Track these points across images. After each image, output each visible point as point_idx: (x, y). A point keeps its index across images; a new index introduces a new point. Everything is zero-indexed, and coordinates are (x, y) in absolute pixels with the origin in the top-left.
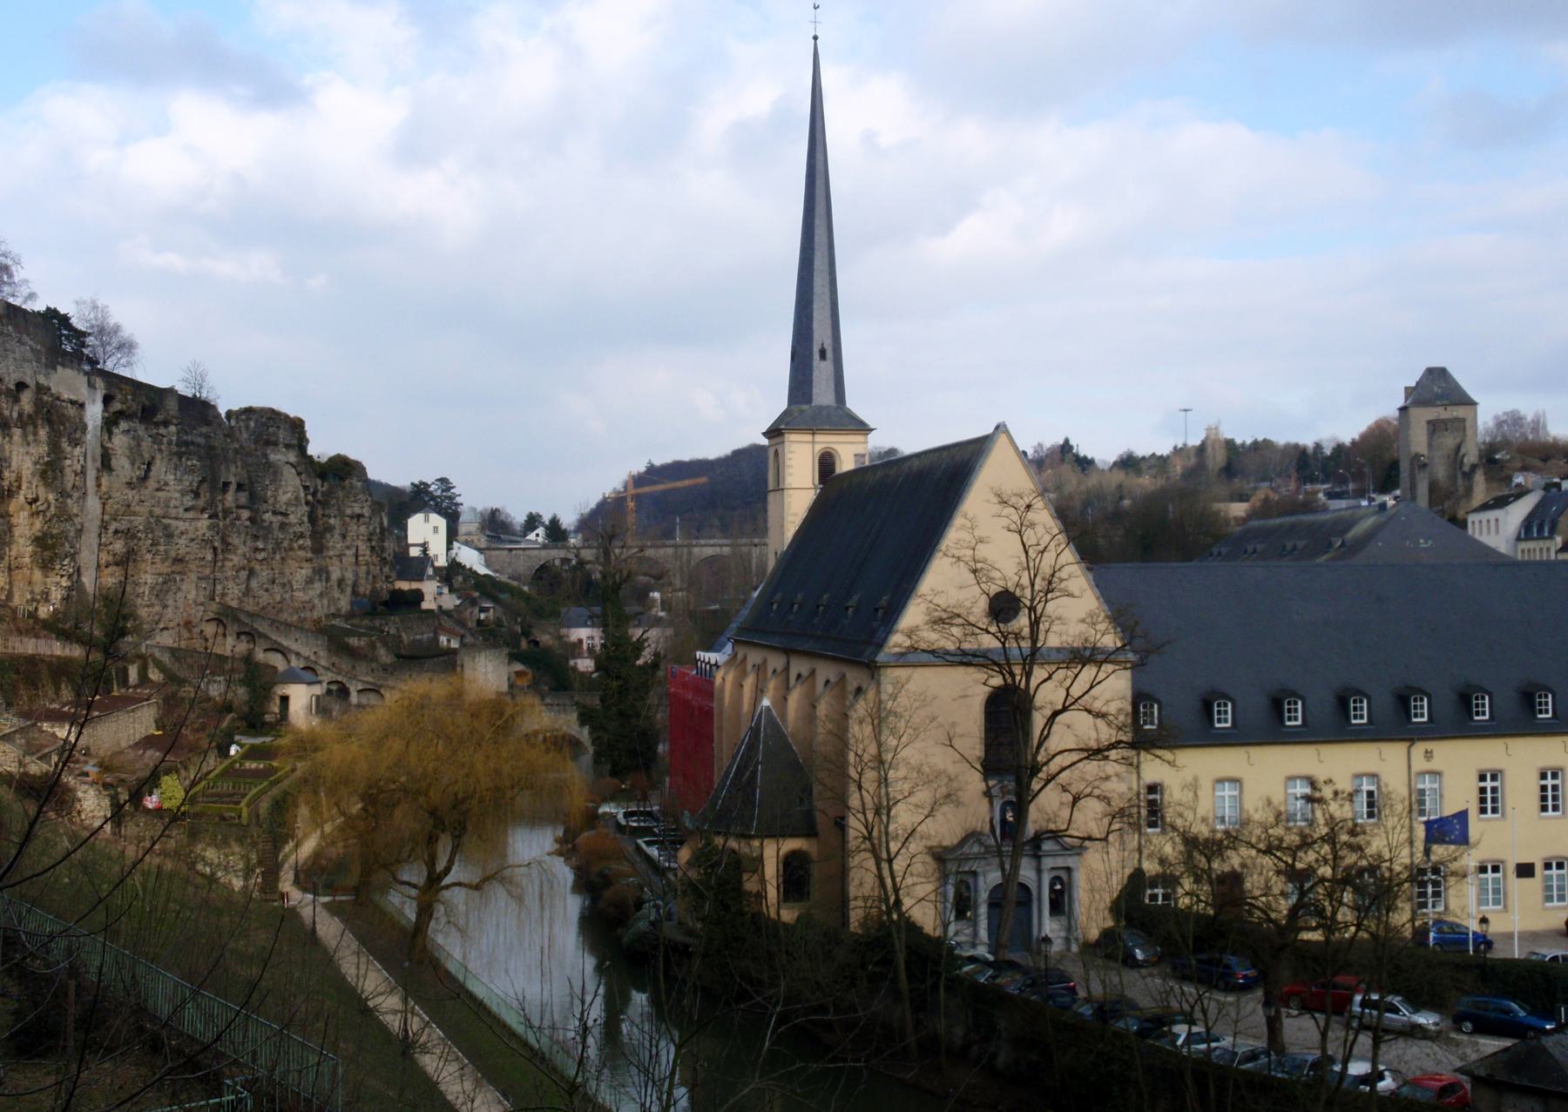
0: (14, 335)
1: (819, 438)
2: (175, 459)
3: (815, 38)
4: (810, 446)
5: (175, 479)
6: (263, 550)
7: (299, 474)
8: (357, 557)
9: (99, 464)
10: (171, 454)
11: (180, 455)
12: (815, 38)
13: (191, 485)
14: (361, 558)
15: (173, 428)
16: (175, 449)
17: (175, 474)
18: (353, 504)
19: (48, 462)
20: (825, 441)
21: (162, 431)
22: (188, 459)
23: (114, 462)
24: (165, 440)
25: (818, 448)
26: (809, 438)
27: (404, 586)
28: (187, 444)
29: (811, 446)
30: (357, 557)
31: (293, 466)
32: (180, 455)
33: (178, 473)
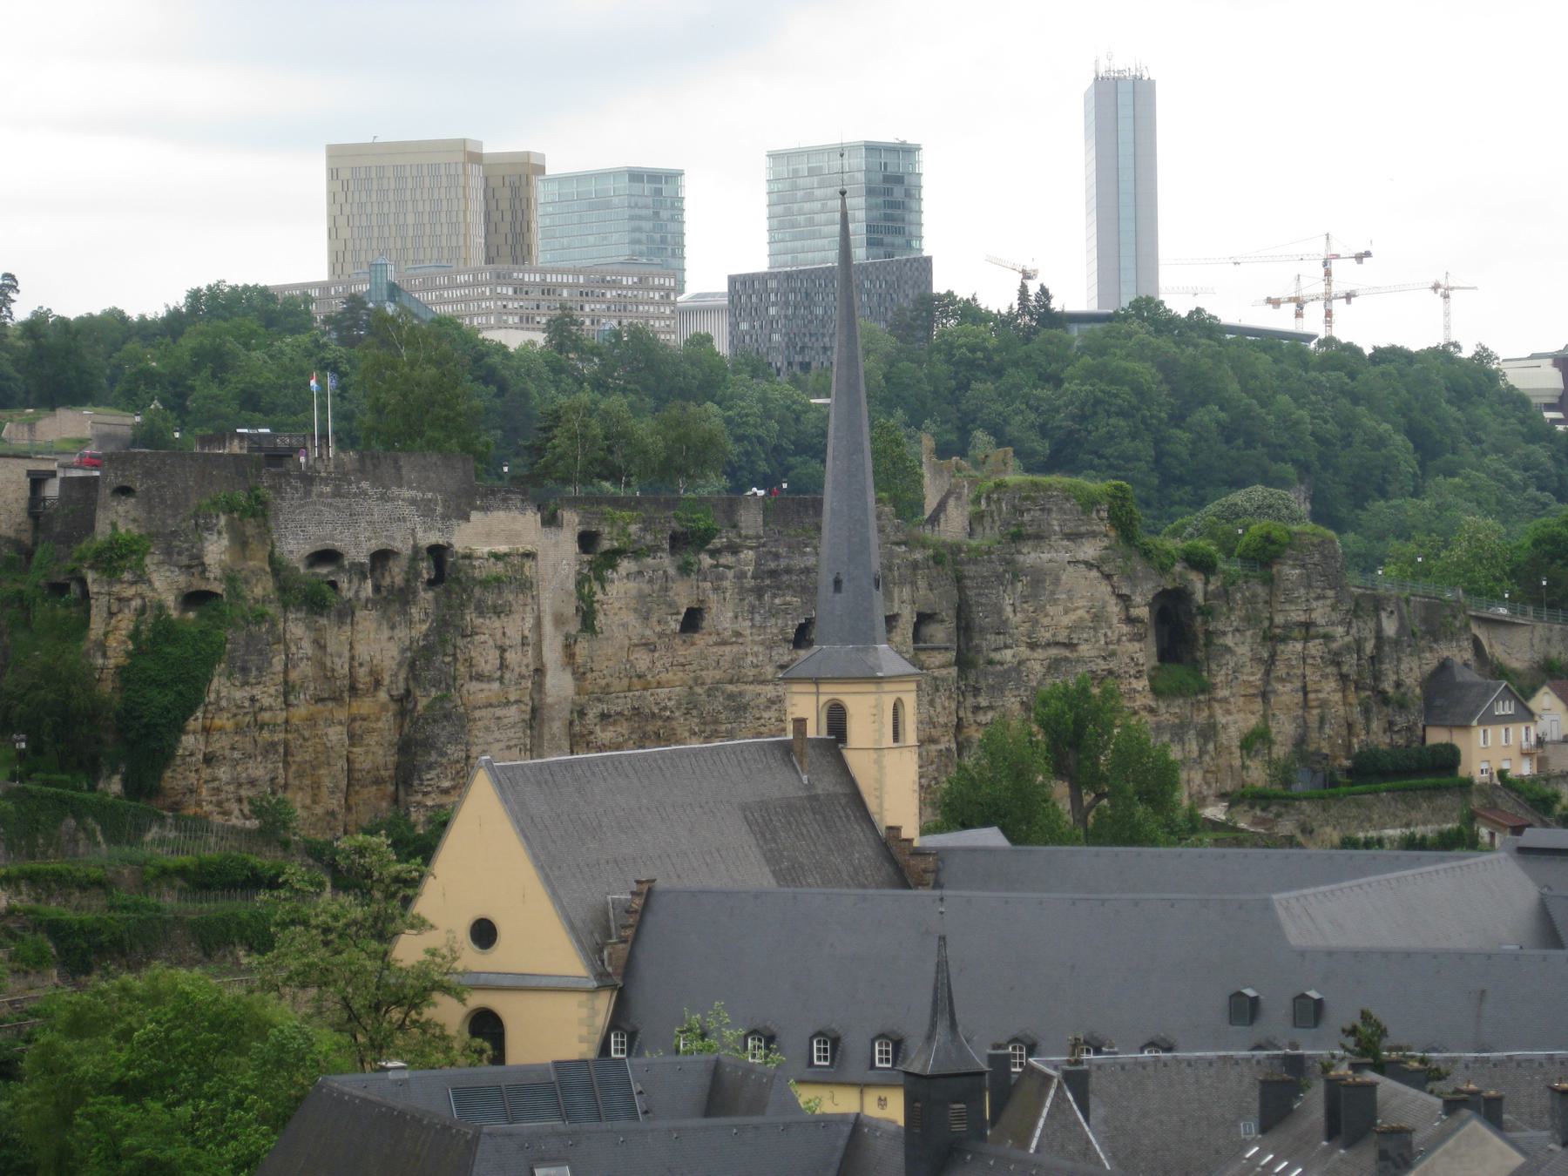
0: (371, 492)
1: (824, 688)
2: (751, 598)
3: (843, 193)
4: (814, 698)
5: (753, 626)
6: (990, 707)
7: (1108, 577)
8: (1306, 694)
9: (574, 627)
10: (742, 591)
11: (759, 592)
12: (843, 193)
13: (782, 631)
14: (1312, 696)
15: (749, 555)
16: (749, 583)
17: (752, 620)
18: (1287, 607)
19: (424, 646)
20: (830, 692)
21: (727, 559)
22: (774, 596)
23: (600, 620)
24: (730, 574)
25: (823, 699)
26: (812, 688)
27: (1436, 736)
28: (773, 574)
29: (814, 697)
30: (1306, 694)
31: (1089, 565)
32: (759, 592)
33: (757, 617)
